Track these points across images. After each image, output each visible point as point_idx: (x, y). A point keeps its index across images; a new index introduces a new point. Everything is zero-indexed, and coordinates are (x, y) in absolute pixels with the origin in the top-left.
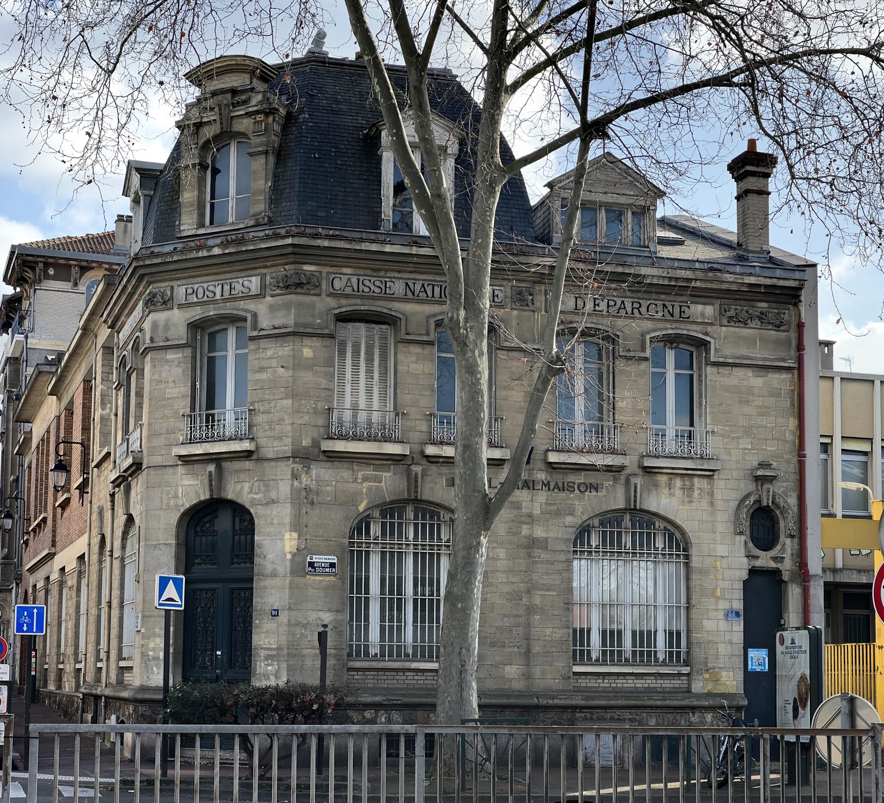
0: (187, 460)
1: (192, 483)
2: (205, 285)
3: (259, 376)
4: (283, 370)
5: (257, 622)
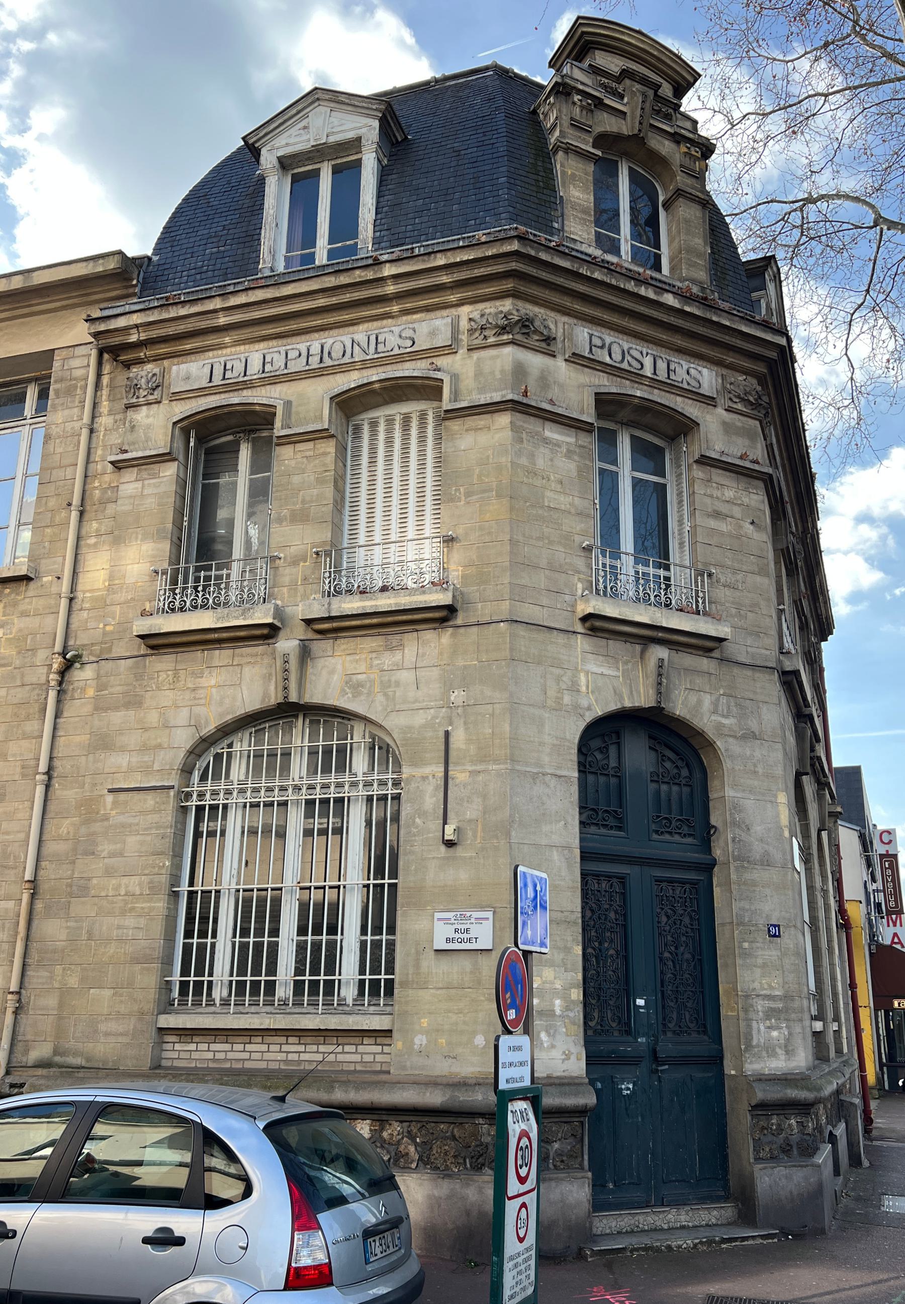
0: (596, 625)
1: (606, 672)
3: (713, 523)
4: (751, 527)
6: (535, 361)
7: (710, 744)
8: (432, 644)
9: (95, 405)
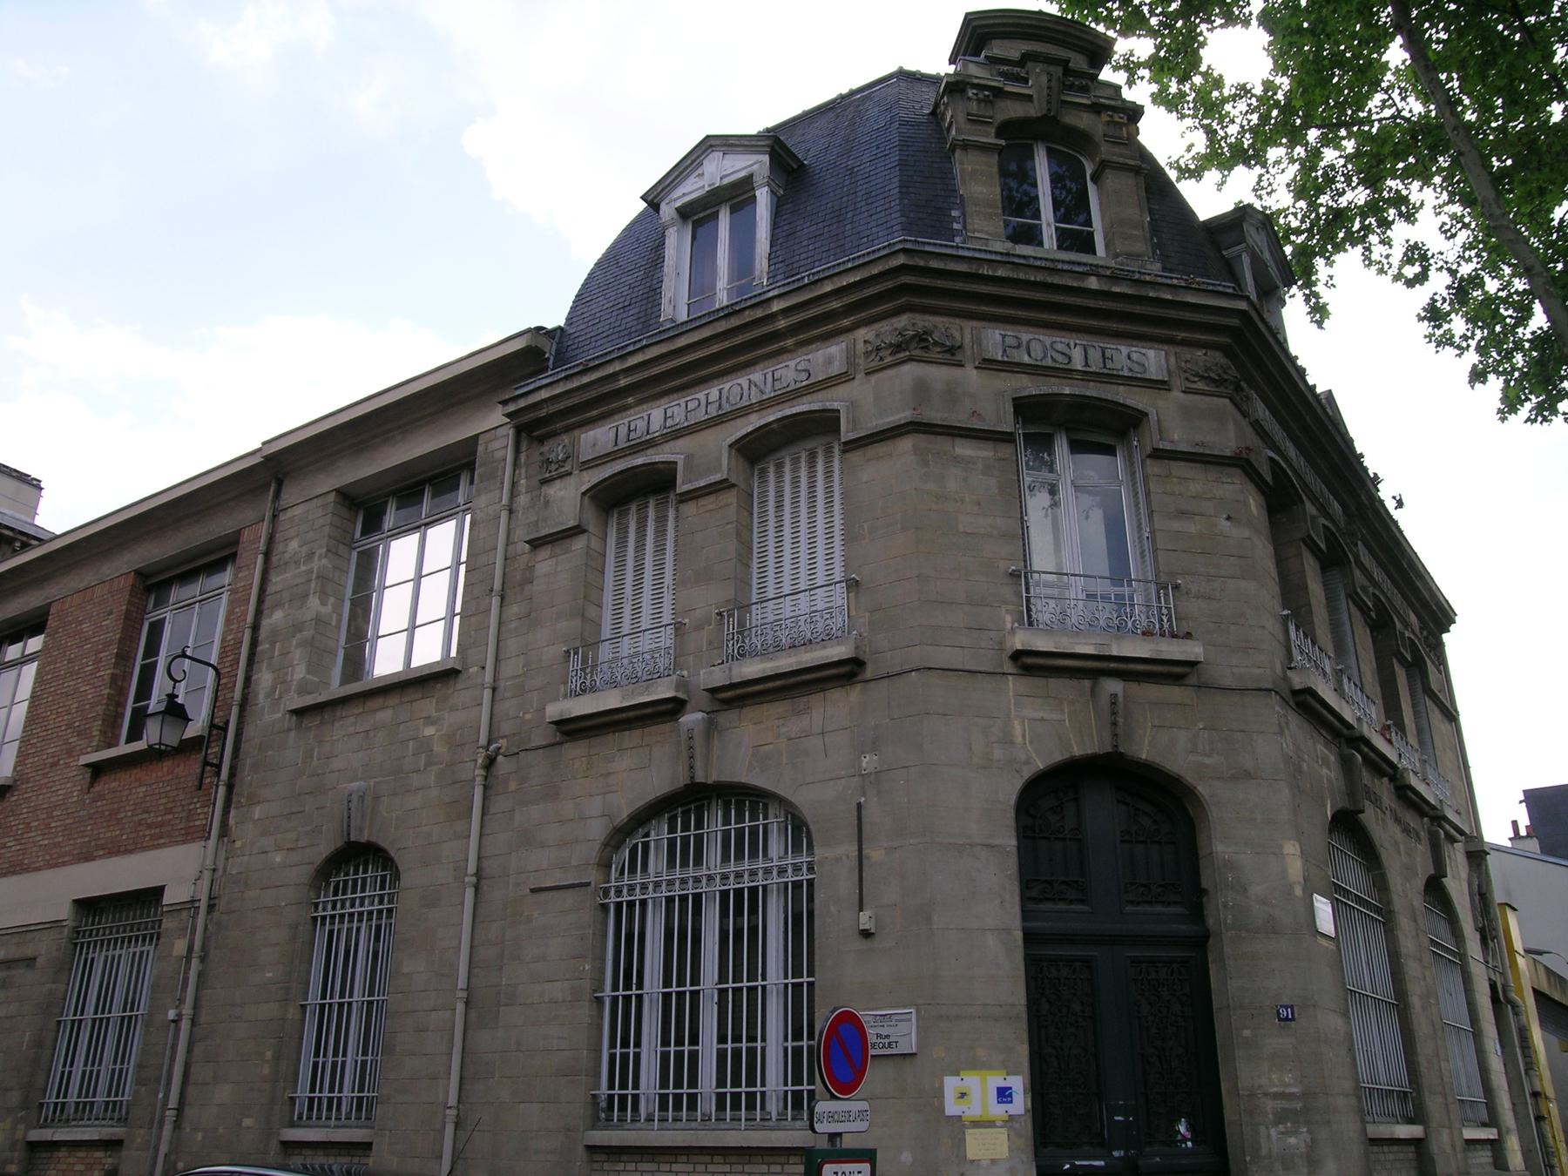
1: (1046, 716)
2: (1047, 340)
3: (1177, 525)
4: (1228, 523)
5: (1247, 1033)
6: (938, 374)
7: (1190, 792)
8: (838, 706)
9: (514, 484)
